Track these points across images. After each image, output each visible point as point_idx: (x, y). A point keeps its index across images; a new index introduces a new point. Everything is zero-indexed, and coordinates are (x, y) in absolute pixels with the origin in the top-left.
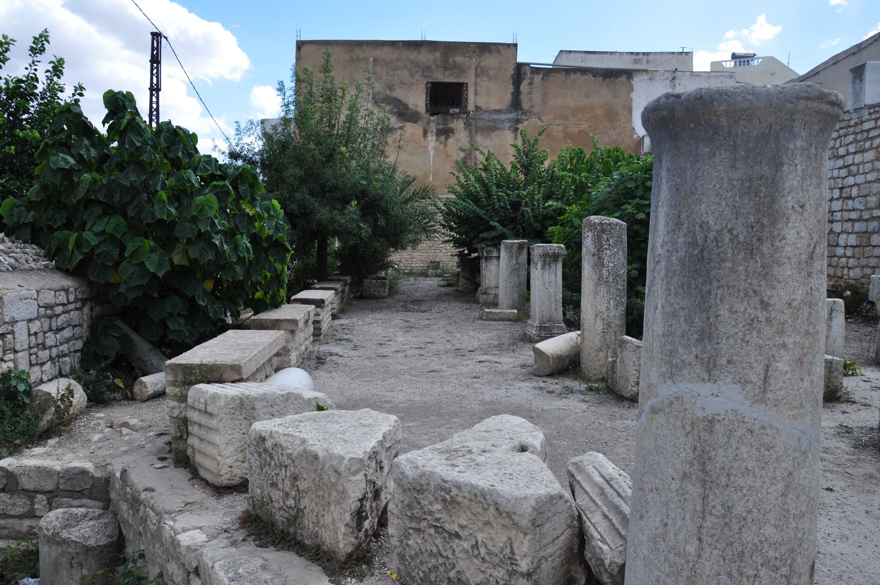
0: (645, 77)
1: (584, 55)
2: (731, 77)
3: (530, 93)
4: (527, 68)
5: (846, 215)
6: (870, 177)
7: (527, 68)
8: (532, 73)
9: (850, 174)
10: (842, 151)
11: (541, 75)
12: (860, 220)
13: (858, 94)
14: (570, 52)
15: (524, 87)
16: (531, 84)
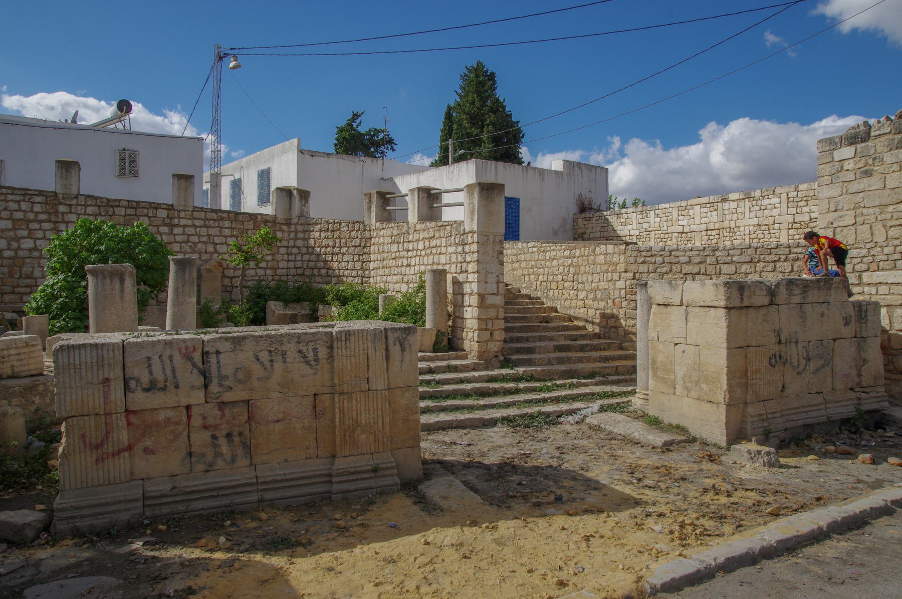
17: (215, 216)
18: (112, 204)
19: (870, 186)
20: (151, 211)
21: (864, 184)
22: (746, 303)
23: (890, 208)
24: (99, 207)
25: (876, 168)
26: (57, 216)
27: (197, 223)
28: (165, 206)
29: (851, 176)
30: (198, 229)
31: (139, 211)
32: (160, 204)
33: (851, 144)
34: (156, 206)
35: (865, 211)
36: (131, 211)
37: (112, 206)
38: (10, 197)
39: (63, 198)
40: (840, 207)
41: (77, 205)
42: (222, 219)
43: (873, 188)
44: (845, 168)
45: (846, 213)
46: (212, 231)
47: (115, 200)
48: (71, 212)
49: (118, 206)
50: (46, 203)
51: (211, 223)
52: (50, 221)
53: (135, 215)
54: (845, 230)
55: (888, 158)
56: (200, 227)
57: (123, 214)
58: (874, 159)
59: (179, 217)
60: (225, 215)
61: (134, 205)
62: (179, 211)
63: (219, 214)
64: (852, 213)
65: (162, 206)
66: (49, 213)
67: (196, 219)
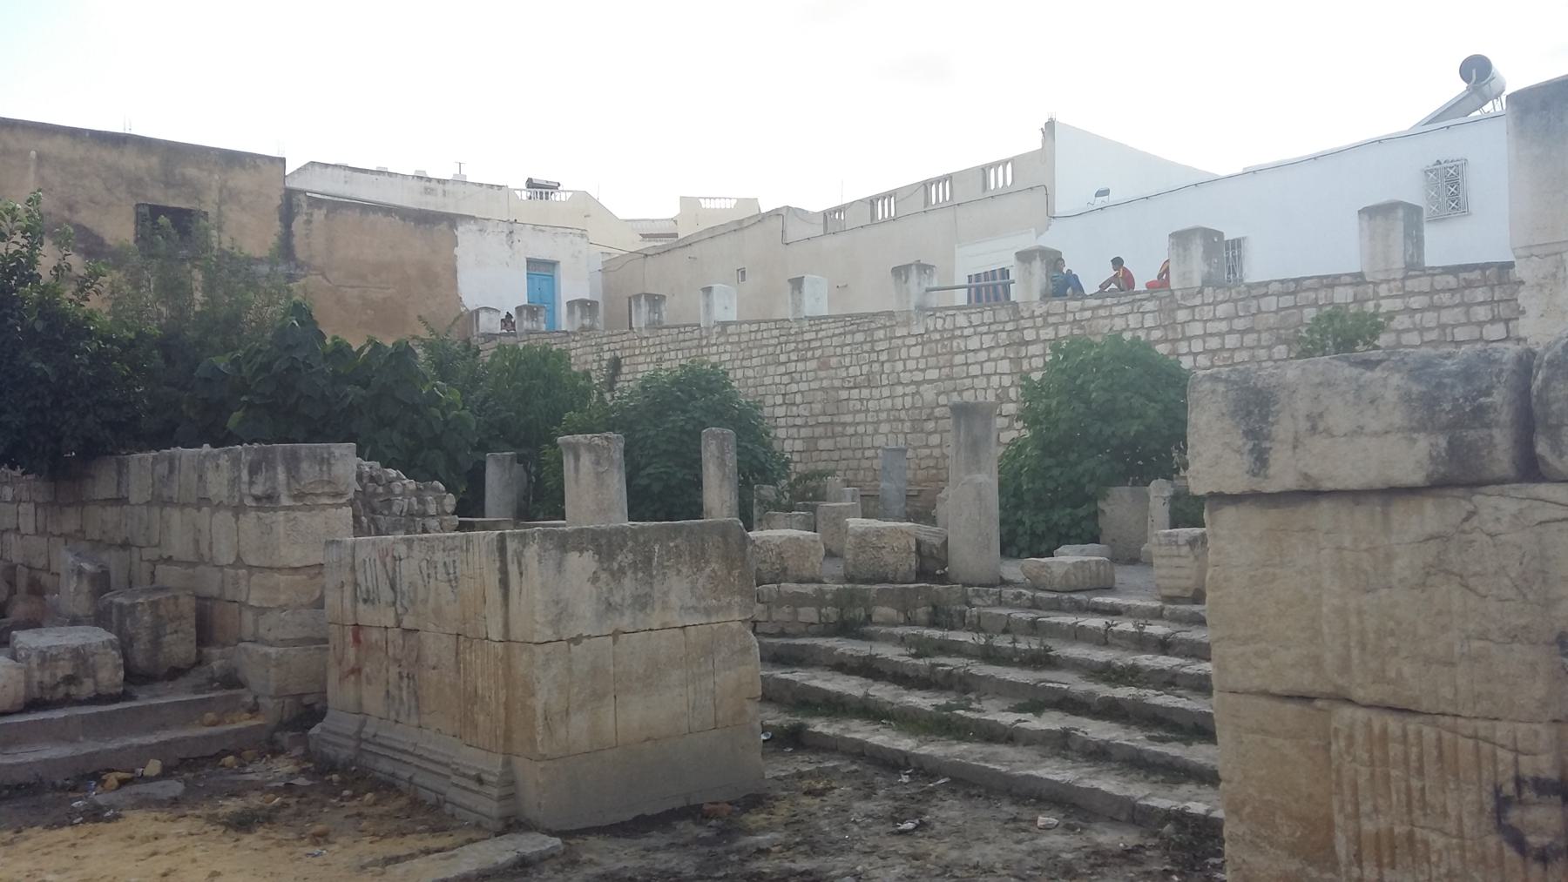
0: (475, 228)
1: (348, 172)
2: (582, 236)
3: (307, 236)
4: (301, 197)
5: (790, 421)
6: (814, 385)
7: (301, 197)
8: (310, 205)
9: (793, 381)
10: (783, 358)
11: (324, 211)
12: (806, 425)
13: (797, 306)
14: (327, 165)
15: (298, 225)
16: (309, 222)
17: (1451, 281)
18: (1254, 292)
20: (1322, 294)
22: (1282, 476)
24: (1235, 301)
26: (1175, 330)
27: (1415, 302)
28: (1348, 279)
30: (1418, 316)
31: (1302, 298)
32: (1338, 277)
34: (1331, 282)
36: (1288, 301)
37: (1254, 297)
38: (1116, 310)
39: (1183, 298)
41: (1203, 304)
42: (1469, 285)
46: (1447, 317)
47: (1260, 284)
48: (1194, 320)
49: (1266, 295)
50: (1160, 311)
51: (1446, 298)
52: (1166, 341)
53: (1295, 306)
56: (1422, 310)
57: (1274, 308)
59: (1376, 296)
60: (1476, 275)
61: (1292, 286)
62: (1376, 284)
63: (1462, 275)
65: (1343, 280)
66: (1165, 327)
67: (1412, 294)
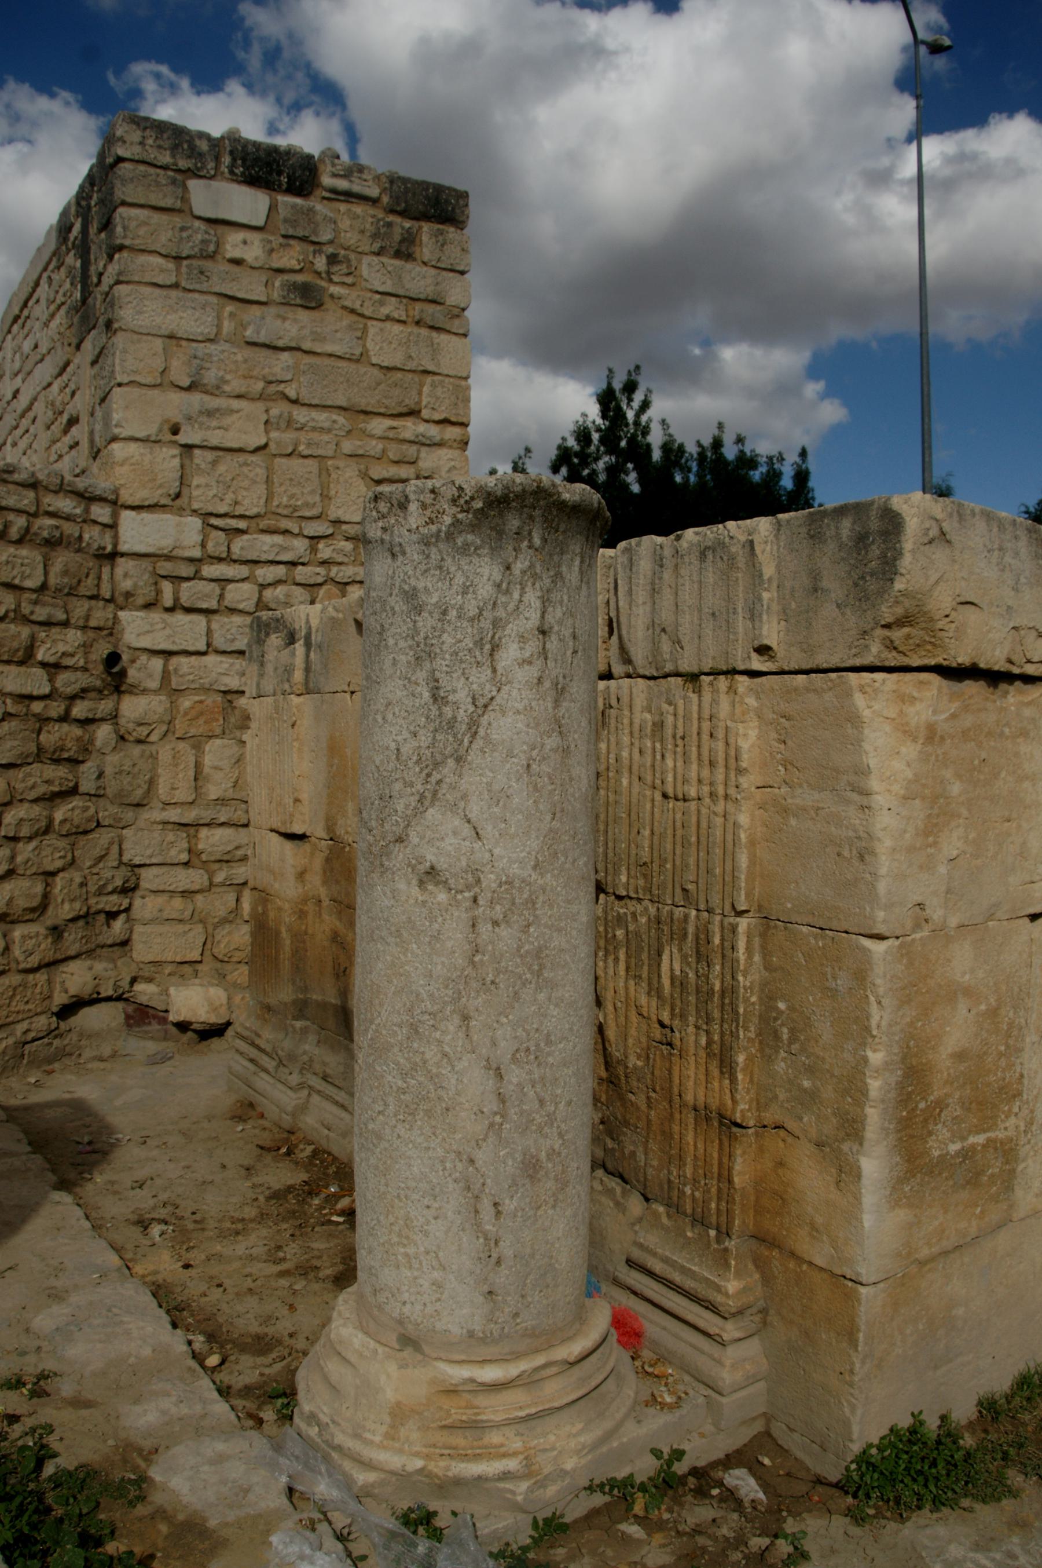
19: (318, 338)
21: (295, 326)
23: (378, 426)
25: (334, 289)
29: (252, 287)
33: (252, 181)
35: (301, 415)
40: (210, 377)
43: (329, 348)
44: (232, 252)
45: (235, 404)
54: (228, 465)
55: (375, 272)
58: (333, 260)
64: (257, 409)
